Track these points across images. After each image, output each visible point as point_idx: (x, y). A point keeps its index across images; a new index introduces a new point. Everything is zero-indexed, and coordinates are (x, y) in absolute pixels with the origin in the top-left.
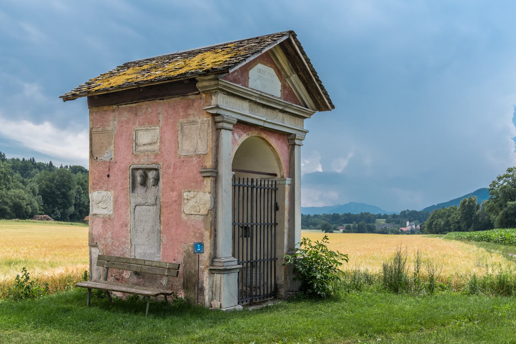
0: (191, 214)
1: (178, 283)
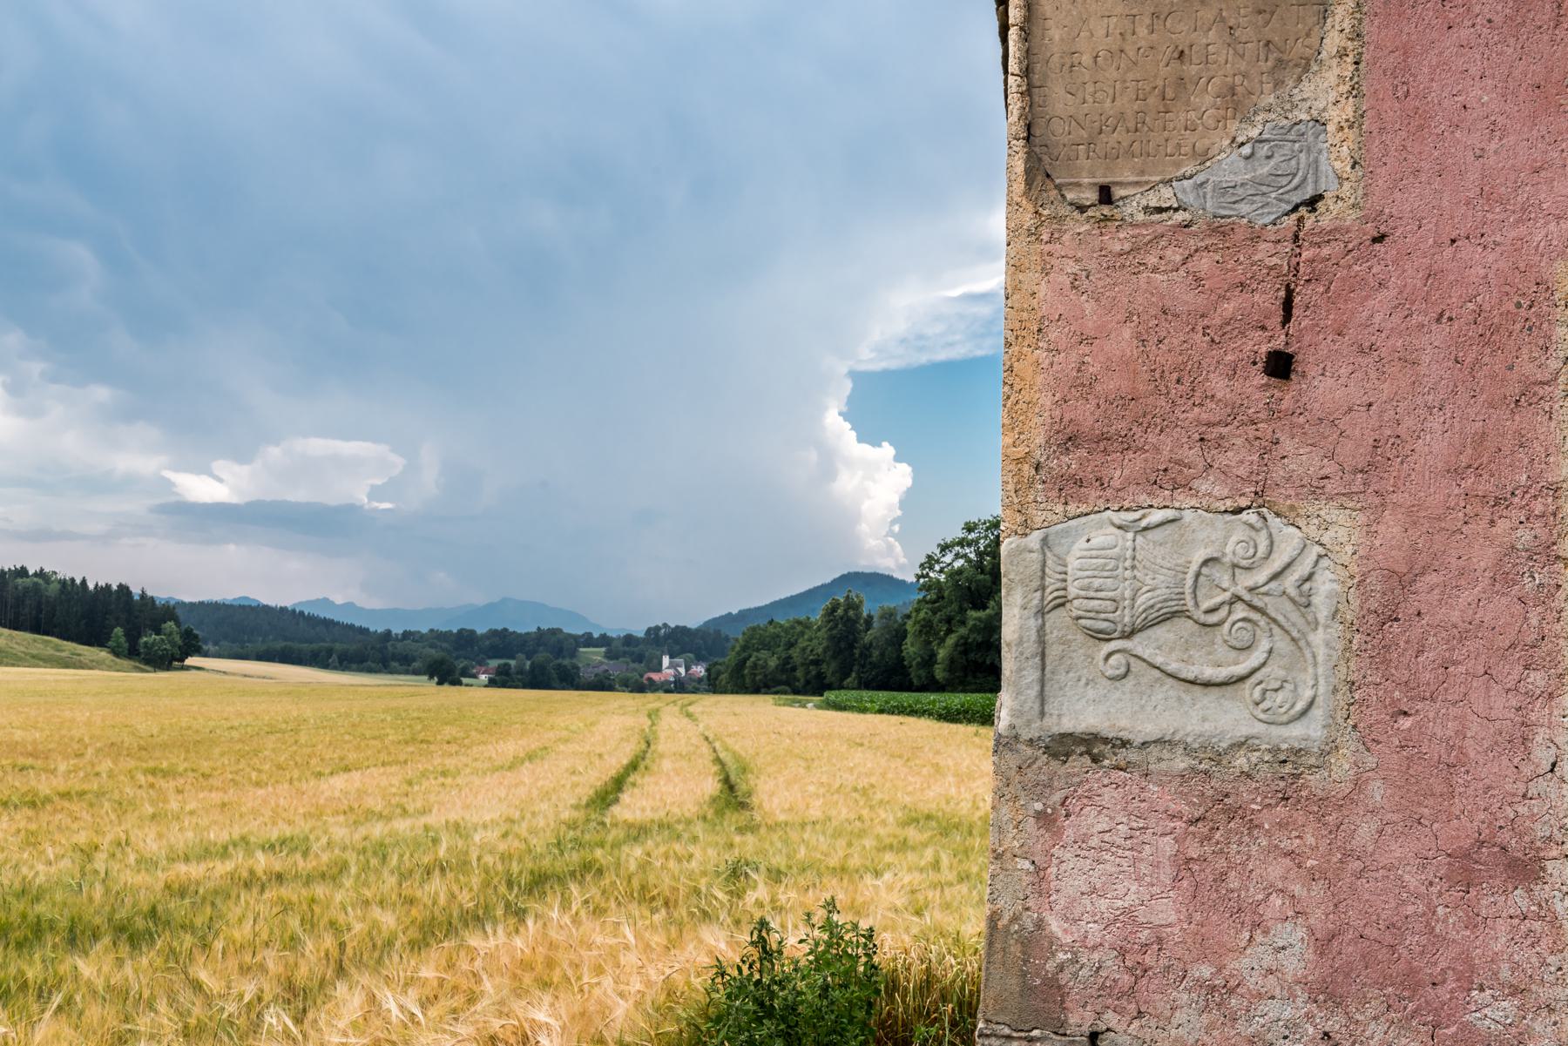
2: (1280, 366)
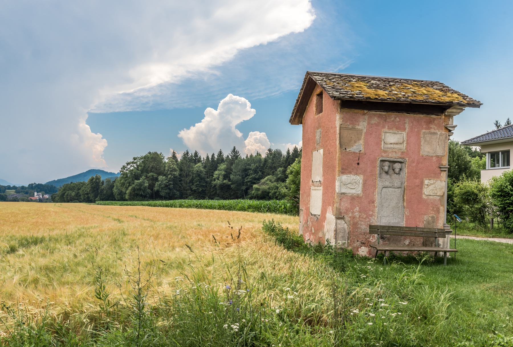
1: (419, 242)
2: (358, 164)
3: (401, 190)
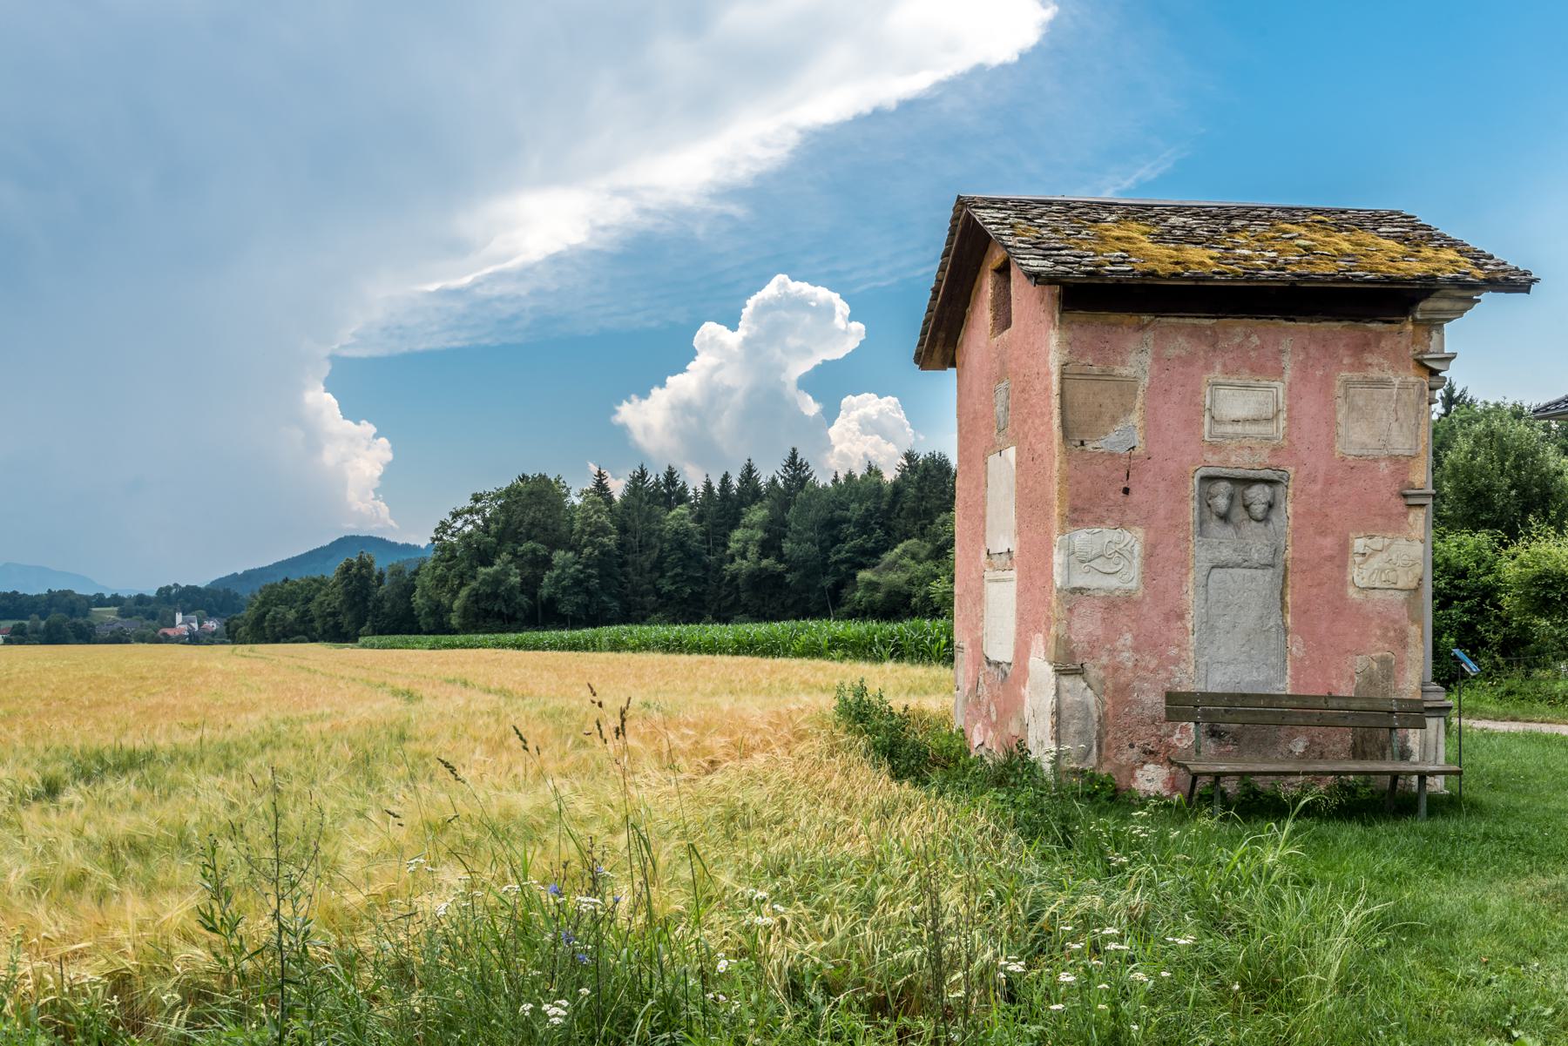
0: (1374, 588)
1: (1339, 746)
2: (1126, 491)
3: (1274, 574)
